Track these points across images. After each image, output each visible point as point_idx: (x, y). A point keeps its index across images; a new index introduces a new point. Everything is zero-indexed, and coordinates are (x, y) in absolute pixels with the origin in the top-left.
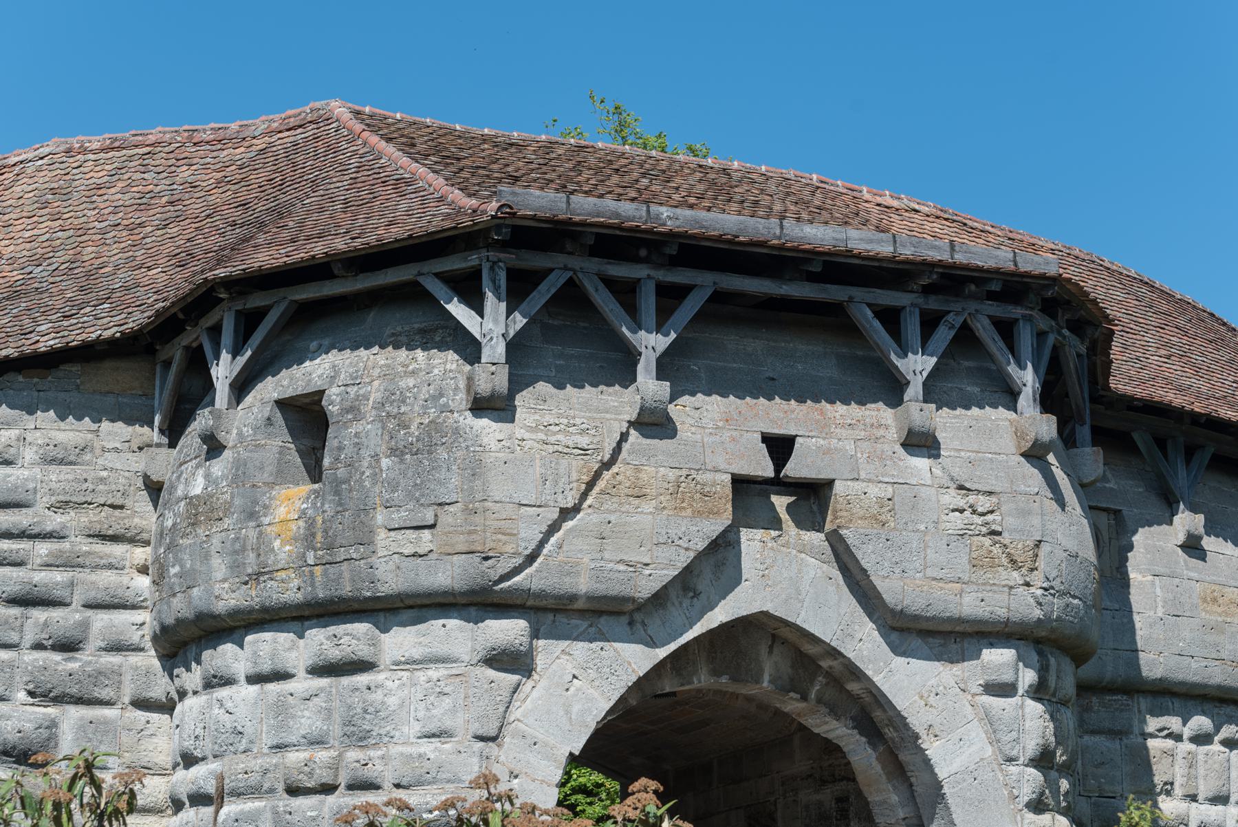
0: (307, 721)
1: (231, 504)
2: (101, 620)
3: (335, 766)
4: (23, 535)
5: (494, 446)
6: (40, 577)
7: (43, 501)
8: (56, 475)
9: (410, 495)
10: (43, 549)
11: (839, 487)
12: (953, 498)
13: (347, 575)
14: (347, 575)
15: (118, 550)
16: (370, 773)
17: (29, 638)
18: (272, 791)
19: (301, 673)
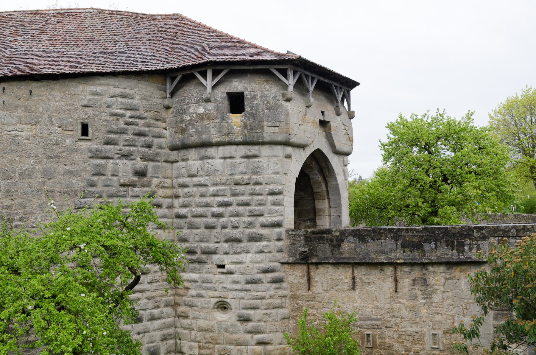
0: (241, 168)
1: (217, 116)
2: (156, 140)
3: (250, 179)
4: (138, 118)
5: (290, 110)
6: (142, 129)
7: (142, 109)
8: (144, 103)
9: (273, 119)
10: (142, 122)
11: (331, 123)
12: (343, 127)
13: (256, 136)
14: (256, 136)
15: (159, 123)
16: (260, 181)
17: (141, 144)
18: (230, 184)
19: (238, 157)
